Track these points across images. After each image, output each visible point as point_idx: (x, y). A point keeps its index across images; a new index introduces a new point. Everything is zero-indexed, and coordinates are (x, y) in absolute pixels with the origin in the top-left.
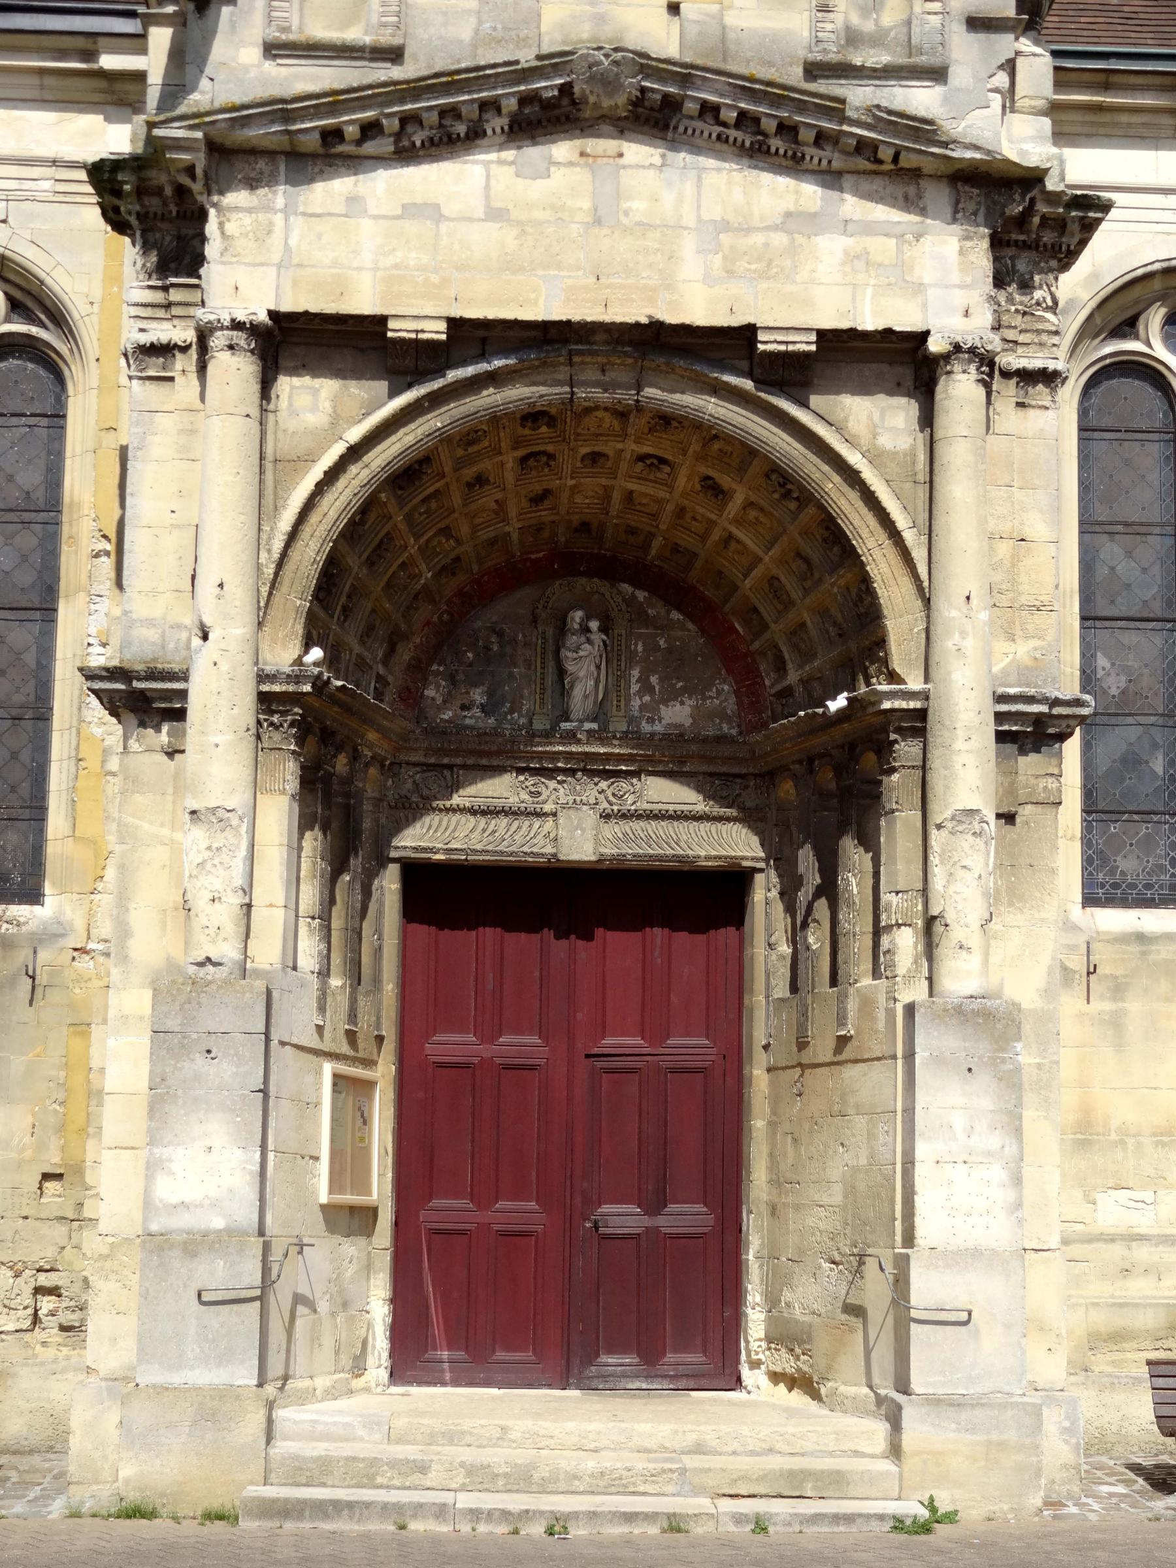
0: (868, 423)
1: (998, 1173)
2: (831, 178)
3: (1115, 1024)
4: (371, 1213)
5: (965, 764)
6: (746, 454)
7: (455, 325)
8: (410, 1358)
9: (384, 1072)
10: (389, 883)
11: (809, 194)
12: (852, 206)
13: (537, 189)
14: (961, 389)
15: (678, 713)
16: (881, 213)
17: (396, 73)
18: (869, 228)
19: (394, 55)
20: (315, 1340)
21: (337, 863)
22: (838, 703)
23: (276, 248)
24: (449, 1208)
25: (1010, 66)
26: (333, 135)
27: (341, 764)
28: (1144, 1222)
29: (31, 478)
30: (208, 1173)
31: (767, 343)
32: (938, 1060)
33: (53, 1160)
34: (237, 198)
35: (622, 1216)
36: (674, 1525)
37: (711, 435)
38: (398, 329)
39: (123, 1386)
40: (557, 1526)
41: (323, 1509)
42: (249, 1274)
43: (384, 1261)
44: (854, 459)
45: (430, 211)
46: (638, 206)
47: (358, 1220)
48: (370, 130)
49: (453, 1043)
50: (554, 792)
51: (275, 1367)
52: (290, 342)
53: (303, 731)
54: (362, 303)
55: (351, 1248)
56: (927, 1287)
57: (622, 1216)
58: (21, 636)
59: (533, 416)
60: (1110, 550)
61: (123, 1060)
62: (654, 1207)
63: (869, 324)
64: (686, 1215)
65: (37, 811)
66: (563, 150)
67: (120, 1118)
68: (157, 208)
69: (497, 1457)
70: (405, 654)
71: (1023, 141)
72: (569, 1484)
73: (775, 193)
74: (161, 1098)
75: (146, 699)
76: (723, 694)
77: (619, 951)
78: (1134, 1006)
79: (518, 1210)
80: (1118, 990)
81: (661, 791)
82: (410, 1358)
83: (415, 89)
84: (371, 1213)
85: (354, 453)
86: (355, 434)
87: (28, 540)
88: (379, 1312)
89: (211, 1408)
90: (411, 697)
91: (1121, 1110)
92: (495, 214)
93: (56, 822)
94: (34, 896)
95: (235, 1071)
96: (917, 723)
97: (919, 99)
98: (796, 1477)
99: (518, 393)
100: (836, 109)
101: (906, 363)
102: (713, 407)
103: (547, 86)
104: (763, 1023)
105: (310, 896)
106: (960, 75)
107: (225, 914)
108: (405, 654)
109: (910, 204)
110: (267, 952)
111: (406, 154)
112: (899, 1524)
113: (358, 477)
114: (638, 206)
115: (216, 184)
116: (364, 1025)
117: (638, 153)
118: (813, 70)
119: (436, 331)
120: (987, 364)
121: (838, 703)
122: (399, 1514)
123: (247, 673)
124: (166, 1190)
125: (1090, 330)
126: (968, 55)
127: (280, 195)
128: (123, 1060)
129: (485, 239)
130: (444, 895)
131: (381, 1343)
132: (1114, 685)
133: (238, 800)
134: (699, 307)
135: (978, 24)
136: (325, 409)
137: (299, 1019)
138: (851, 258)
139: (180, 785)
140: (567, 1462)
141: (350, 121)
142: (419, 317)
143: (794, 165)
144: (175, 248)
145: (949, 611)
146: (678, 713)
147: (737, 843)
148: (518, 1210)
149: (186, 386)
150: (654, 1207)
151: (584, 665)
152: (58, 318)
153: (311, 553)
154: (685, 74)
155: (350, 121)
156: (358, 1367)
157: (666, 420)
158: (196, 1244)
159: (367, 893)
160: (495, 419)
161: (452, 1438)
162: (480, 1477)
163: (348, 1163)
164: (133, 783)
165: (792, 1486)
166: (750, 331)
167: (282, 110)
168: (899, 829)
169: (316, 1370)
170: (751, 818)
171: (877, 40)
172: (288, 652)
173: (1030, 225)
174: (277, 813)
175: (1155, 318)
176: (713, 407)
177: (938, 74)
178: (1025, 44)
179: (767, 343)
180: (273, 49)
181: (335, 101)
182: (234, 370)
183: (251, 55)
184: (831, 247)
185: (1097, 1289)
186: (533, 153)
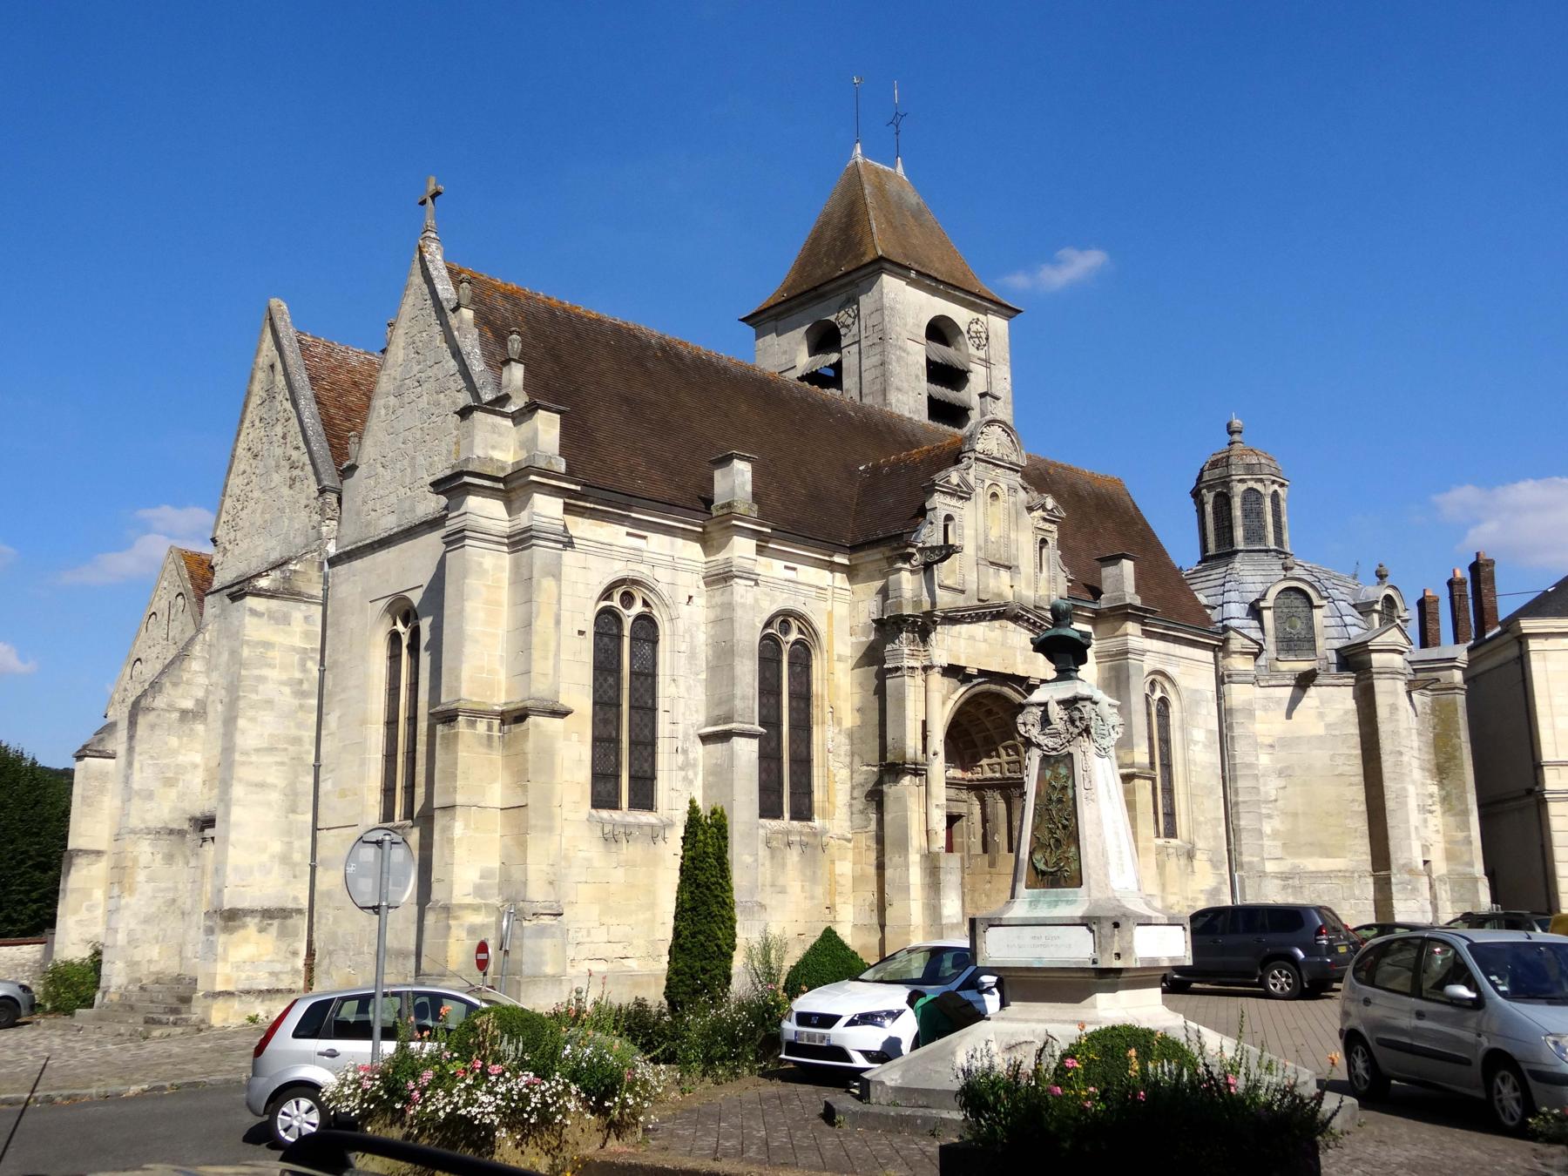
33: (828, 903)
45: (972, 638)
119: (975, 672)
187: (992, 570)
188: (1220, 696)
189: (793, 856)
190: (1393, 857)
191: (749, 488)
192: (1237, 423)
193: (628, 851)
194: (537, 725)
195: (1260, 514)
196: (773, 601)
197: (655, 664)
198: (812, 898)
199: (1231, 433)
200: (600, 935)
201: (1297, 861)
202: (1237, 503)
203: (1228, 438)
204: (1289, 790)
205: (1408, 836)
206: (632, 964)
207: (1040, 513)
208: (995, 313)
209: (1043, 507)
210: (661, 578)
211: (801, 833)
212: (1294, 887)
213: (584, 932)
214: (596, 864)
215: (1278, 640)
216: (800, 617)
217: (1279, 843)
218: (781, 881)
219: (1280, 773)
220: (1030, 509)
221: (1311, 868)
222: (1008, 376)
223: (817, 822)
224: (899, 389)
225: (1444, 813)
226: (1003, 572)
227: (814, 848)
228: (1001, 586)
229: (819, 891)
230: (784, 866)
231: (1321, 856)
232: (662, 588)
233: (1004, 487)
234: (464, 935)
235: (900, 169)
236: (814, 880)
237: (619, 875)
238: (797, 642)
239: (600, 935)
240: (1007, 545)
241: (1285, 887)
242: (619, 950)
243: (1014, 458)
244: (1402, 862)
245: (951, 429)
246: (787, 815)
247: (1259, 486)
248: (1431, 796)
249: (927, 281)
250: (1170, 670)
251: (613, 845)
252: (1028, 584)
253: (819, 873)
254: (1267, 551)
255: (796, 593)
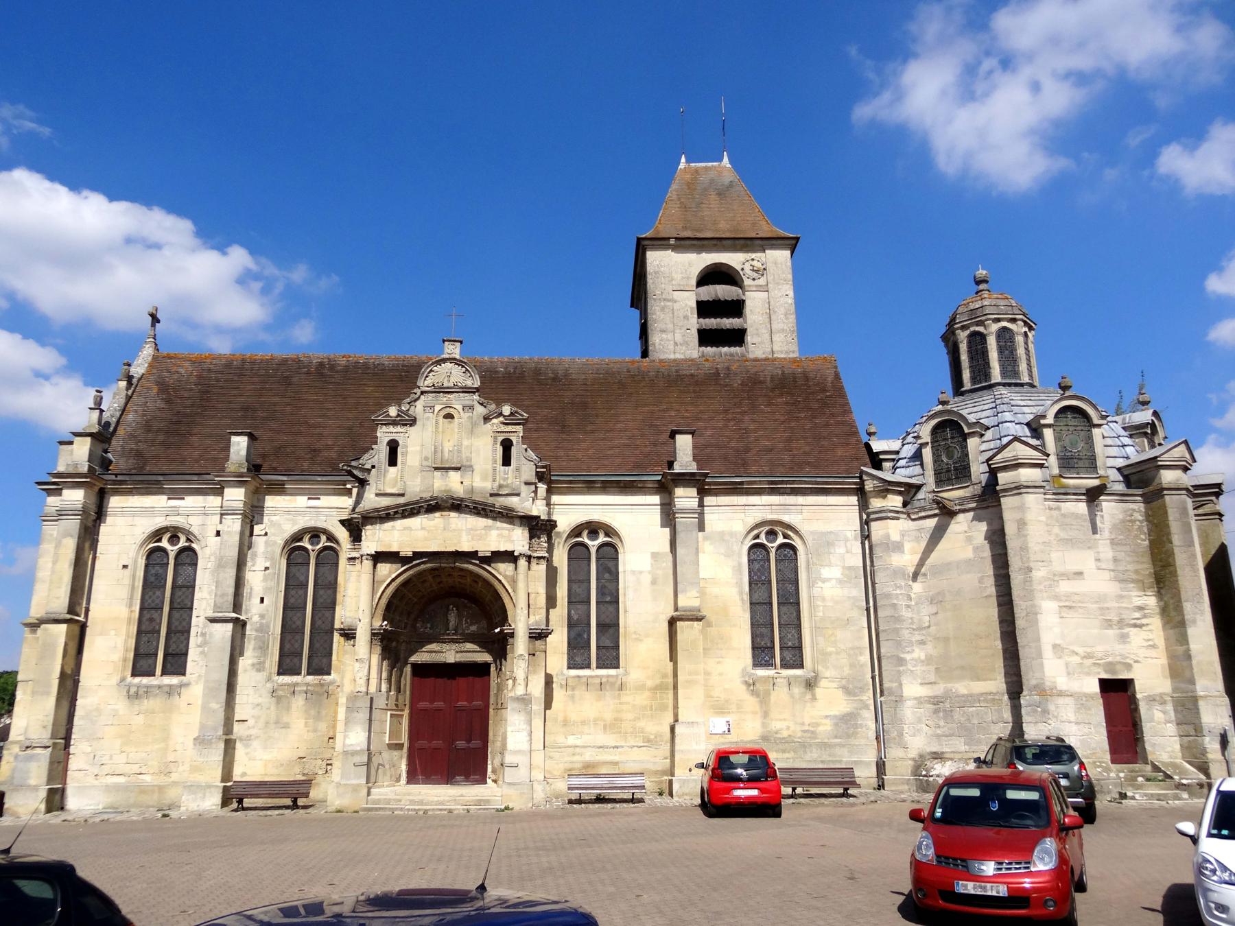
0: (503, 570)
1: (525, 734)
2: (494, 519)
3: (572, 697)
4: (402, 745)
5: (520, 645)
6: (479, 576)
7: (414, 553)
8: (412, 778)
9: (406, 713)
10: (408, 669)
11: (490, 522)
12: (499, 524)
13: (432, 523)
14: (522, 562)
15: (474, 628)
16: (505, 525)
17: (401, 500)
18: (503, 529)
19: (403, 495)
20: (384, 774)
21: (392, 667)
22: (497, 630)
23: (376, 538)
24: (422, 743)
25: (536, 492)
26: (388, 514)
27: (394, 644)
28: (579, 742)
29: (331, 578)
30: (356, 738)
31: (480, 554)
32: (513, 709)
34: (369, 527)
35: (461, 744)
36: (450, 811)
37: (471, 572)
38: (402, 554)
39: (339, 785)
40: (426, 812)
41: (377, 809)
42: (365, 759)
43: (405, 756)
44: (500, 577)
45: (409, 528)
46: (453, 526)
47: (399, 746)
48: (396, 513)
49: (423, 705)
50: (446, 647)
51: (372, 779)
52: (379, 557)
53: (382, 641)
54: (394, 549)
55: (396, 753)
56: (508, 759)
57: (461, 744)
58: (327, 614)
59: (433, 569)
60: (575, 586)
61: (341, 714)
62: (469, 741)
63: (502, 549)
64: (476, 743)
65: (330, 655)
66: (437, 514)
67: (340, 726)
68: (355, 528)
69: (416, 798)
70: (413, 616)
71: (538, 509)
72: (431, 803)
73: (482, 522)
74: (347, 721)
75: (349, 635)
76: (484, 623)
77: (462, 682)
78: (577, 693)
79: (437, 743)
80: (573, 689)
81: (470, 646)
82: (412, 778)
83: (404, 505)
84: (402, 745)
85: (393, 580)
86: (393, 576)
87: (330, 592)
88: (404, 767)
89: (355, 789)
90: (414, 626)
91: (573, 717)
92: (423, 529)
93: (334, 657)
94: (329, 674)
95: (365, 715)
96: (512, 635)
97: (513, 502)
98: (480, 801)
99: (429, 565)
100: (493, 506)
101: (510, 557)
102: (470, 567)
103: (433, 503)
104: (492, 700)
105: (384, 675)
106: (523, 495)
107: (363, 682)
108: (413, 616)
109: (512, 523)
110: (373, 689)
111: (404, 517)
112: (497, 810)
113: (394, 585)
114: (453, 526)
115: (364, 524)
116: (400, 701)
117: (453, 514)
118: (492, 495)
119: (410, 554)
120: (529, 558)
121: (497, 630)
122: (393, 810)
123: (369, 629)
124: (348, 742)
125: (569, 536)
126: (526, 491)
127: (378, 526)
128: (341, 714)
129: (421, 534)
130: (421, 671)
131: (404, 775)
132: (575, 617)
133: (366, 657)
134: (466, 547)
135: (526, 484)
136: (387, 571)
137: (381, 702)
138: (498, 535)
139: (355, 653)
140: (431, 799)
141: (391, 512)
142: (407, 551)
143: (486, 516)
144: (356, 537)
145: (519, 611)
146: (474, 628)
147: (487, 657)
148: (437, 743)
149: (358, 566)
150: (469, 741)
151: (452, 620)
152: (337, 542)
153: (384, 601)
154: (462, 500)
155: (391, 512)
156: (398, 780)
157: (462, 570)
158: (354, 753)
159: (402, 672)
160: (425, 571)
161: (409, 794)
162: (412, 802)
163: (394, 733)
164: (345, 652)
165: (479, 803)
166: (477, 552)
167: (377, 510)
168: (509, 657)
169: (384, 779)
170: (489, 652)
171: (507, 486)
172: (378, 623)
173: (539, 528)
174: (375, 659)
175: (585, 533)
176: (470, 567)
177: (518, 495)
178: (540, 485)
179: (480, 554)
180: (377, 495)
181: (388, 508)
182: (368, 564)
183: (373, 496)
184: (494, 533)
185: (567, 759)
186: (431, 515)
187: (438, 474)
188: (866, 536)
189: (299, 702)
190: (1024, 681)
191: (244, 453)
192: (982, 273)
193: (147, 704)
194: (46, 630)
195: (984, 353)
196: (295, 523)
197: (195, 580)
198: (315, 731)
199: (978, 283)
200: (122, 759)
201: (949, 685)
202: (963, 347)
203: (976, 288)
204: (940, 616)
205: (1040, 655)
206: (147, 778)
207: (501, 419)
208: (773, 247)
209: (501, 414)
210: (193, 523)
211: (308, 685)
212: (945, 711)
213: (107, 757)
214: (121, 712)
215: (937, 473)
216: (325, 531)
217: (932, 668)
218: (285, 719)
219: (932, 601)
220: (487, 419)
221: (964, 691)
222: (791, 294)
223: (333, 676)
224: (663, 331)
225: (1164, 626)
226: (452, 473)
227: (322, 696)
228: (454, 484)
229: (322, 726)
230: (288, 709)
231: (972, 680)
232: (195, 530)
233: (459, 407)
234: (12, 759)
235: (726, 161)
236: (318, 717)
237: (140, 720)
238: (325, 548)
239: (122, 759)
240: (459, 451)
241: (936, 712)
242: (136, 769)
243: (469, 383)
244: (1033, 682)
245: (733, 350)
246: (304, 671)
247: (981, 329)
248: (1140, 608)
249: (685, 243)
250: (786, 518)
251: (137, 702)
252: (484, 478)
253: (324, 713)
254: (1022, 385)
255: (318, 514)
